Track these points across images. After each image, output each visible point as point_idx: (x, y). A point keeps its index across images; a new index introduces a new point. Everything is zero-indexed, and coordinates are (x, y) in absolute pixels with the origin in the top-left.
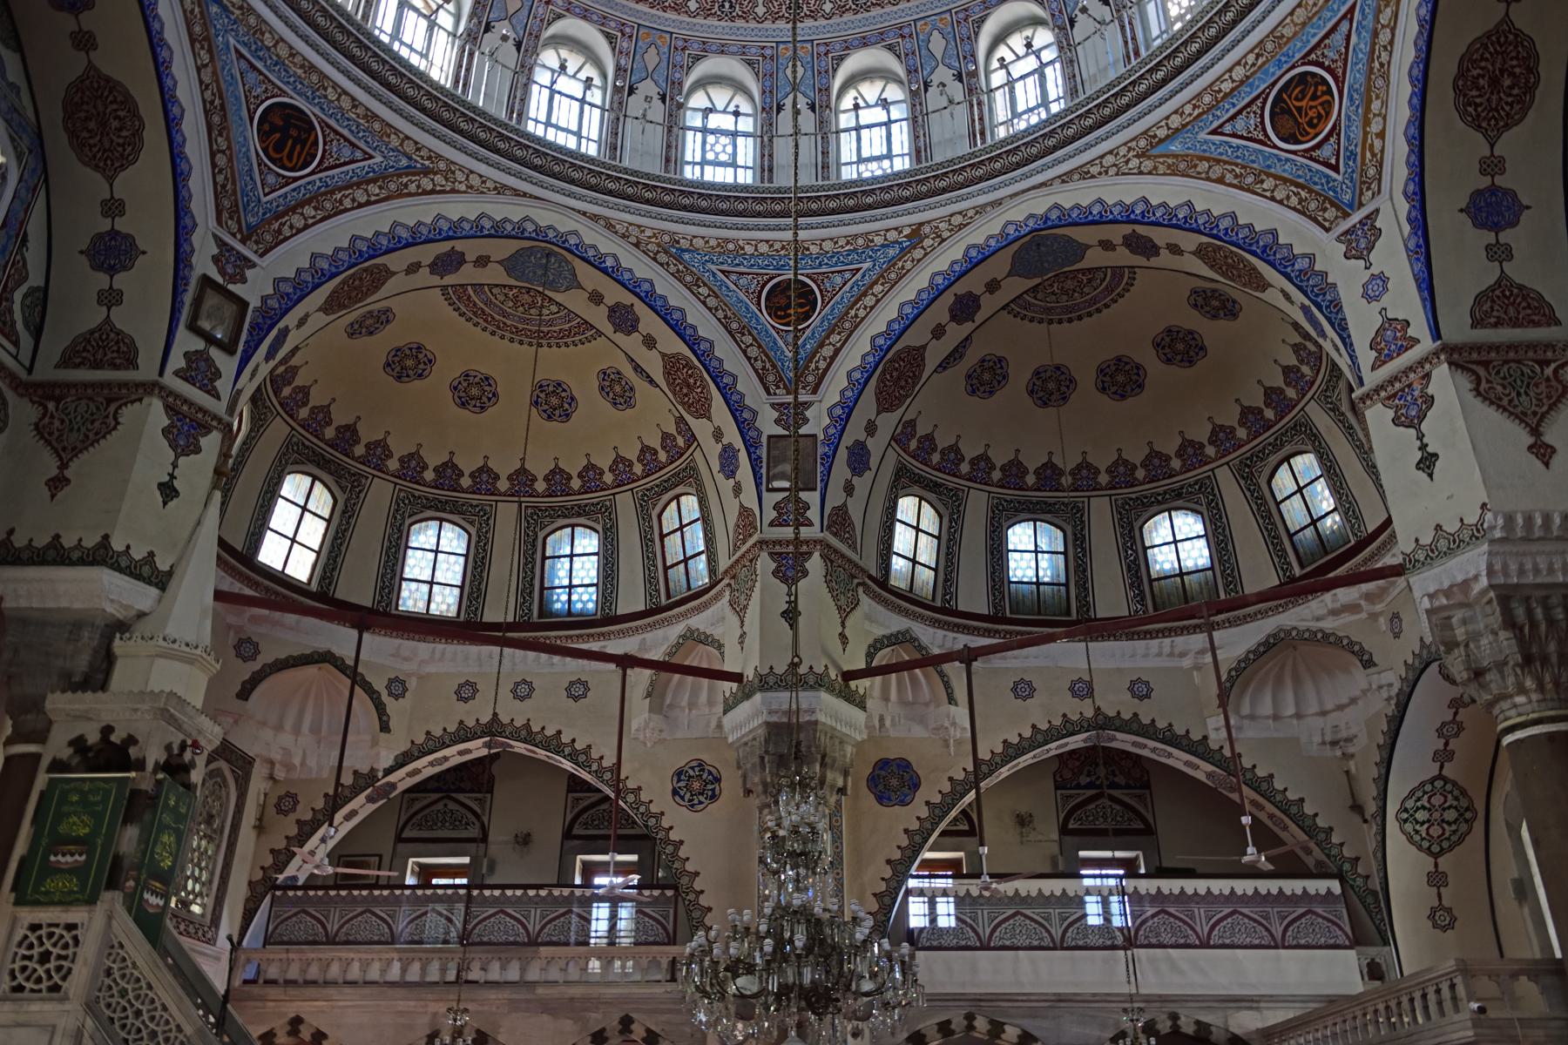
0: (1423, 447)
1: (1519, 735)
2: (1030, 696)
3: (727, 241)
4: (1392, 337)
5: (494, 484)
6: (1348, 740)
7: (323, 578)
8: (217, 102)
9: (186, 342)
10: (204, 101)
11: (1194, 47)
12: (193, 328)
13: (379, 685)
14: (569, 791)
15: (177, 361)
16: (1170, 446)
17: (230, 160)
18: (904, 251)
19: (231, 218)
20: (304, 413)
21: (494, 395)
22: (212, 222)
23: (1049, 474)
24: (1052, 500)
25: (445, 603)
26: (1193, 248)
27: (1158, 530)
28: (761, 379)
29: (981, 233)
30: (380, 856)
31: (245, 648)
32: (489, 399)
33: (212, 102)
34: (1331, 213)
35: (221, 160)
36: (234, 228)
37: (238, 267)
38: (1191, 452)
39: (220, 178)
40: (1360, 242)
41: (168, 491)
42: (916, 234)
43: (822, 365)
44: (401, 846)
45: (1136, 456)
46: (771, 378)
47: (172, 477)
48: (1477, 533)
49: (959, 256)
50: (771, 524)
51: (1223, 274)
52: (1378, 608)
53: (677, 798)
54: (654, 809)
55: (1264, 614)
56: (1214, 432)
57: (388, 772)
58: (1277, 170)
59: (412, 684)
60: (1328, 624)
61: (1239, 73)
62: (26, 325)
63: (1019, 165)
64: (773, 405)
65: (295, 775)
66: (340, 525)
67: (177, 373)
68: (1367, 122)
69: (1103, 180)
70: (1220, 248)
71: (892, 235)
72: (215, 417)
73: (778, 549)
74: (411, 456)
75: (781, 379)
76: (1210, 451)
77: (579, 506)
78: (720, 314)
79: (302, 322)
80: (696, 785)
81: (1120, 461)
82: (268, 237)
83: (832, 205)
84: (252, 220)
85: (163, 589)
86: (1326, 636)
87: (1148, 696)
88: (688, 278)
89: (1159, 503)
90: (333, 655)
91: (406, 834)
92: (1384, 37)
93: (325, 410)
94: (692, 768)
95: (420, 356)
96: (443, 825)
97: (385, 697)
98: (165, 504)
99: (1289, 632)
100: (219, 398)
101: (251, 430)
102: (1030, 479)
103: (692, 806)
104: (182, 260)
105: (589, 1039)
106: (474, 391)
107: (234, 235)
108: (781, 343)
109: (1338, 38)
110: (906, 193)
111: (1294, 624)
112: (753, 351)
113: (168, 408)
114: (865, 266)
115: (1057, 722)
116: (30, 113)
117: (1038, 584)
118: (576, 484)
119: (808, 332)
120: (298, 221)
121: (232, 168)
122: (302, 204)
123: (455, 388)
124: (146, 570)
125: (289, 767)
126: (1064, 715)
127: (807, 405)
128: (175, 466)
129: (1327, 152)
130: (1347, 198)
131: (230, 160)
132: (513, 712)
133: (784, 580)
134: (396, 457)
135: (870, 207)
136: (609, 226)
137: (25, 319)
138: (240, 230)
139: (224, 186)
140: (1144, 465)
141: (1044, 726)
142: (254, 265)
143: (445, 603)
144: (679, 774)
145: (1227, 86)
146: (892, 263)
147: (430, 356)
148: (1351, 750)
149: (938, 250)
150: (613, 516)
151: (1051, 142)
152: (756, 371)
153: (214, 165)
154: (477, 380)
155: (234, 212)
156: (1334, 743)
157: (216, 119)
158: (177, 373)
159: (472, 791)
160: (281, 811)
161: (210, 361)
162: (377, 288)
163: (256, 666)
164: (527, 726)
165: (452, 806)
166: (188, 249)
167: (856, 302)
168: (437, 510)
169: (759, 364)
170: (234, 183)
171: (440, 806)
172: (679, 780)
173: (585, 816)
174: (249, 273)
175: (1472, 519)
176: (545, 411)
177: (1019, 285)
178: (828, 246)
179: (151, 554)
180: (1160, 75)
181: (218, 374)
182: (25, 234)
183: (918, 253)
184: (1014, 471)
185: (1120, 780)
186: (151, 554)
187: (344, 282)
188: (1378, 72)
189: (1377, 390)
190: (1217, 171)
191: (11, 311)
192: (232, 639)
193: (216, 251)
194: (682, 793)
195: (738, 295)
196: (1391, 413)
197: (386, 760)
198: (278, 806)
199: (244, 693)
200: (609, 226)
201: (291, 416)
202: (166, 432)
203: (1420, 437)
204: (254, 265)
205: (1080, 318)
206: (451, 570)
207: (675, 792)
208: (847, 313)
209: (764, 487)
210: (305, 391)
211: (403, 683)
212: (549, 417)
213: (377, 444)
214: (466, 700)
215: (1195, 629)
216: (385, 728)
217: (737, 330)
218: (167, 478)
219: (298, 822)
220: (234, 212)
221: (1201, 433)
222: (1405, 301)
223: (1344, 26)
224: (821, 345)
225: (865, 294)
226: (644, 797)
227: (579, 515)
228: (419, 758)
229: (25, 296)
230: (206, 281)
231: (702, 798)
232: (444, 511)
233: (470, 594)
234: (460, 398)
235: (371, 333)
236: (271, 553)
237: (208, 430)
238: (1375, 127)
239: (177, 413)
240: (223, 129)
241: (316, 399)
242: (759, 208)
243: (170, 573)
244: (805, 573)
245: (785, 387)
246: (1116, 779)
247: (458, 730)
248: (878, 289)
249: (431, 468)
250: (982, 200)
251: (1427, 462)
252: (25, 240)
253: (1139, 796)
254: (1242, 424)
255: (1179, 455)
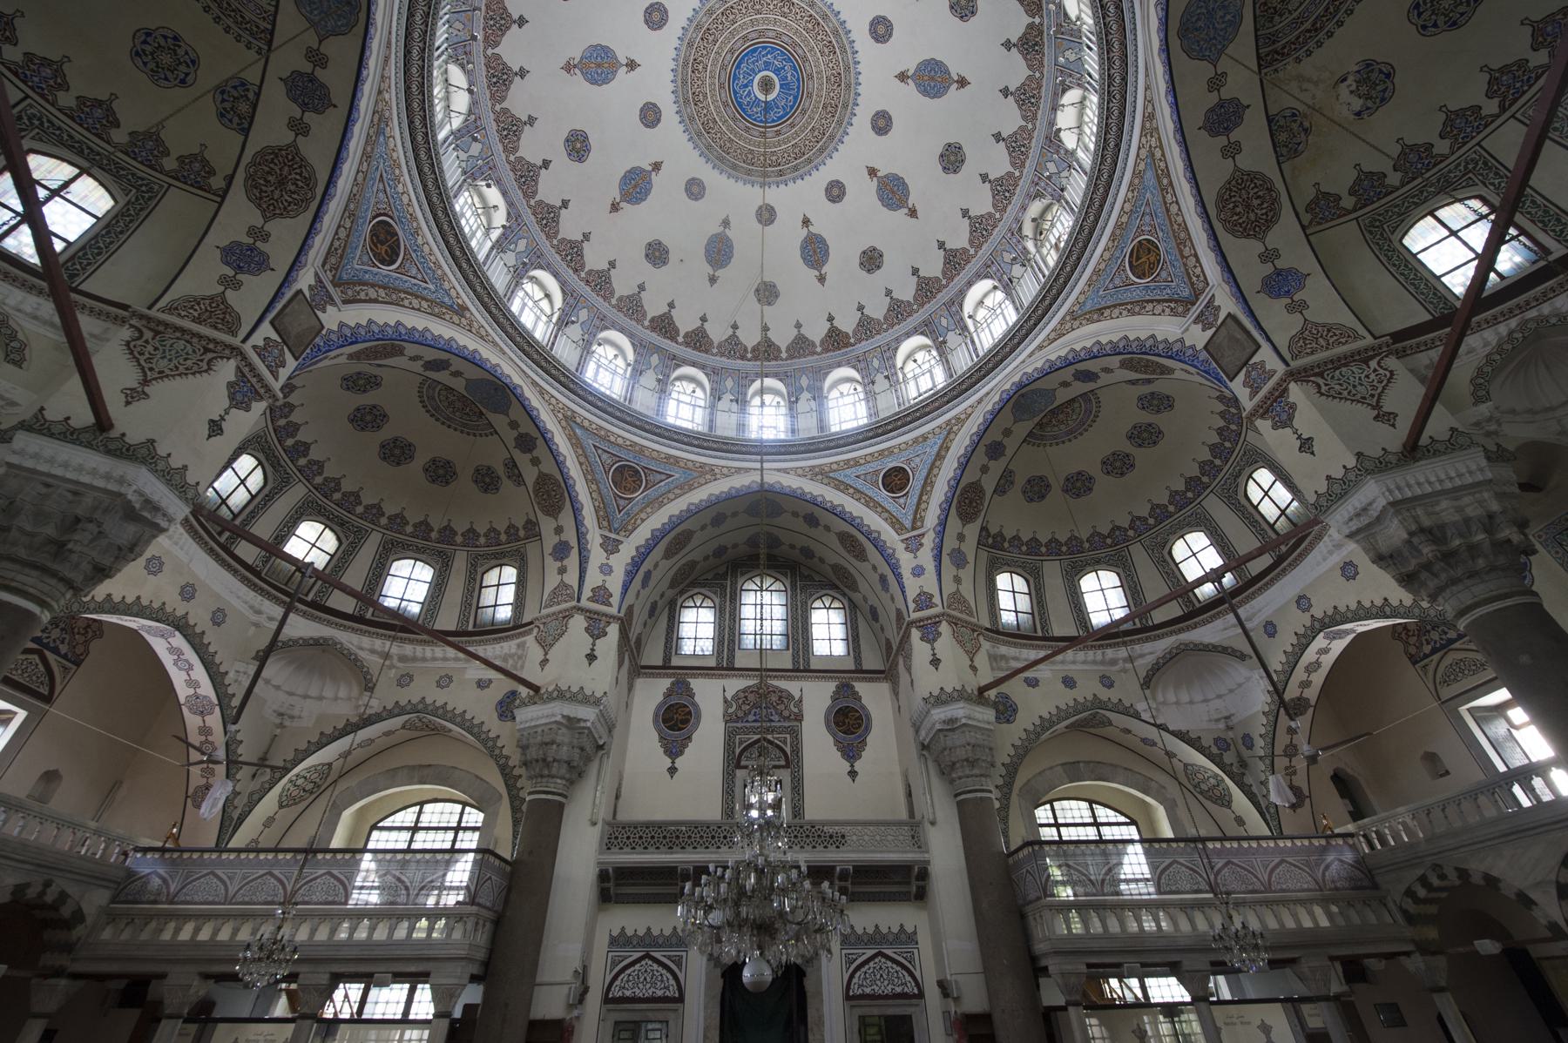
0: (593, 650)
1: (543, 796)
2: (155, 574)
3: (399, 167)
4: (601, 594)
6: (292, 717)
11: (618, 414)
16: (368, 499)
18: (450, 308)
23: (302, 449)
24: (283, 463)
26: (545, 471)
27: (309, 530)
28: (328, 253)
29: (488, 354)
34: (605, 523)
38: (375, 512)
40: (611, 547)
42: (461, 310)
43: (362, 296)
45: (347, 486)
46: (333, 260)
48: (597, 702)
49: (446, 337)
50: (254, 347)
51: (536, 492)
52: (400, 665)
55: (329, 623)
56: (397, 516)
58: (602, 487)
60: (362, 654)
61: (620, 441)
63: (523, 351)
64: (316, 274)
68: (641, 511)
69: (545, 405)
70: (560, 486)
71: (453, 293)
73: (246, 370)
75: (336, 269)
76: (384, 521)
78: (355, 189)
81: (337, 482)
83: (452, 240)
86: (356, 659)
87: (219, 625)
88: (369, 149)
89: (328, 519)
92: (671, 496)
99: (336, 644)
102: (290, 442)
108: (358, 253)
109: (659, 477)
110: (478, 288)
111: (343, 641)
112: (343, 234)
114: (432, 287)
115: (156, 605)
117: (224, 501)
119: (375, 269)
126: (164, 604)
127: (332, 302)
129: (622, 502)
130: (616, 526)
133: (232, 397)
135: (460, 268)
136: (387, 59)
140: (344, 495)
141: (145, 602)
145: (612, 439)
146: (442, 304)
148: (287, 723)
149: (464, 332)
151: (544, 364)
152: (332, 244)
156: (281, 715)
167: (411, 294)
169: (337, 244)
175: (598, 695)
177: (458, 384)
178: (426, 248)
180: (600, 404)
183: (456, 319)
184: (293, 429)
185: (64, 649)
188: (658, 503)
189: (587, 611)
190: (582, 459)
195: (373, 199)
196: (586, 625)
200: (387, 59)
203: (594, 645)
205: (449, 427)
208: (400, 291)
209: (271, 316)
215: (278, 602)
217: (349, 213)
221: (390, 509)
222: (615, 584)
223: (663, 477)
224: (373, 286)
225: (417, 297)
238: (643, 515)
242: (430, 184)
244: (248, 409)
245: (334, 276)
246: (61, 646)
248: (424, 304)
250: (497, 339)
251: (591, 657)
253: (65, 668)
254: (415, 526)
255: (366, 507)
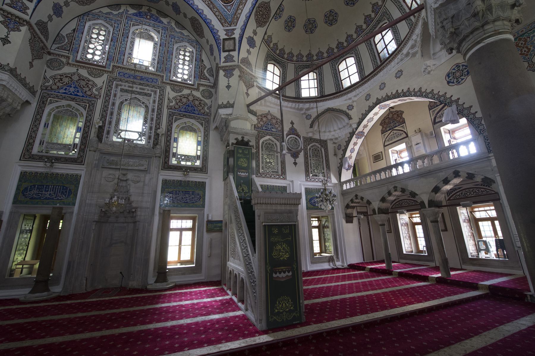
5: (352, 38)
7: (320, 92)
8: (209, 2)
9: (224, 54)
10: (206, 5)
12: (224, 51)
13: (345, 109)
14: (429, 110)
15: (223, 60)
17: (219, 12)
19: (225, 23)
20: (295, 58)
21: (336, 14)
22: (222, 27)
25: (355, 79)
30: (382, 152)
31: (308, 117)
32: (336, 16)
33: (208, 3)
35: (217, 13)
36: (227, 25)
37: (230, 32)
39: (219, 17)
41: (228, 87)
44: (386, 148)
47: (229, 83)
53: (450, 84)
54: (441, 94)
57: (357, 129)
59: (355, 104)
62: (210, 76)
65: (339, 139)
66: (319, 78)
67: (223, 63)
72: (234, 66)
74: (328, 49)
77: (377, 21)
79: (255, 33)
80: (458, 74)
82: (235, 21)
84: (229, 20)
85: (233, 107)
90: (330, 108)
91: (386, 144)
93: (300, 54)
94: (454, 69)
95: (311, 22)
96: (394, 138)
97: (348, 111)
98: (228, 90)
100: (235, 61)
101: (283, 70)
103: (459, 83)
104: (217, 39)
105: (442, 182)
106: (331, 18)
107: (228, 26)
113: (223, 70)
116: (194, 38)
118: (373, 15)
120: (239, 11)
121: (220, 13)
122: (239, 7)
123: (326, 22)
124: (228, 105)
125: (336, 139)
128: (229, 81)
131: (219, 12)
132: (382, 94)
134: (325, 52)
137: (209, 75)
138: (229, 24)
139: (221, 18)
142: (236, 29)
143: (355, 79)
144: (448, 75)
147: (313, 20)
150: (388, 13)
153: (216, 16)
154: (329, 14)
155: (226, 21)
157: (211, 6)
158: (223, 63)
159: (399, 125)
160: (339, 149)
161: (230, 55)
162: (270, 10)
163: (312, 119)
164: (387, 95)
165: (395, 132)
166: (218, 37)
168: (342, 57)
170: (222, 16)
171: (392, 133)
172: (449, 77)
173: (439, 114)
174: (235, 32)
176: (351, 4)
179: (228, 101)
181: (233, 57)
182: (202, 60)
186: (228, 101)
187: (256, 15)
191: (205, 75)
192: (304, 116)
193: (225, 33)
194: (452, 81)
197: (355, 126)
198: (338, 148)
199: (311, 126)
201: (292, 61)
202: (224, 76)
204: (236, 29)
206: (353, 69)
207: (448, 83)
210: (291, 53)
211: (352, 105)
212: (353, 4)
213: (318, 53)
214: (368, 100)
216: (350, 118)
218: (227, 85)
219: (342, 150)
220: (226, 21)
226: (435, 92)
227: (379, 23)
228: (362, 121)
229: (207, 71)
230: (224, 40)
231: (462, 77)
232: (344, 56)
233: (360, 72)
234: (329, 24)
235: (294, 27)
236: (305, 94)
237: (234, 69)
239: (226, 70)
240: (214, 7)
241: (295, 53)
243: (234, 103)
247: (369, 109)
249: (335, 48)
252: (202, 61)
